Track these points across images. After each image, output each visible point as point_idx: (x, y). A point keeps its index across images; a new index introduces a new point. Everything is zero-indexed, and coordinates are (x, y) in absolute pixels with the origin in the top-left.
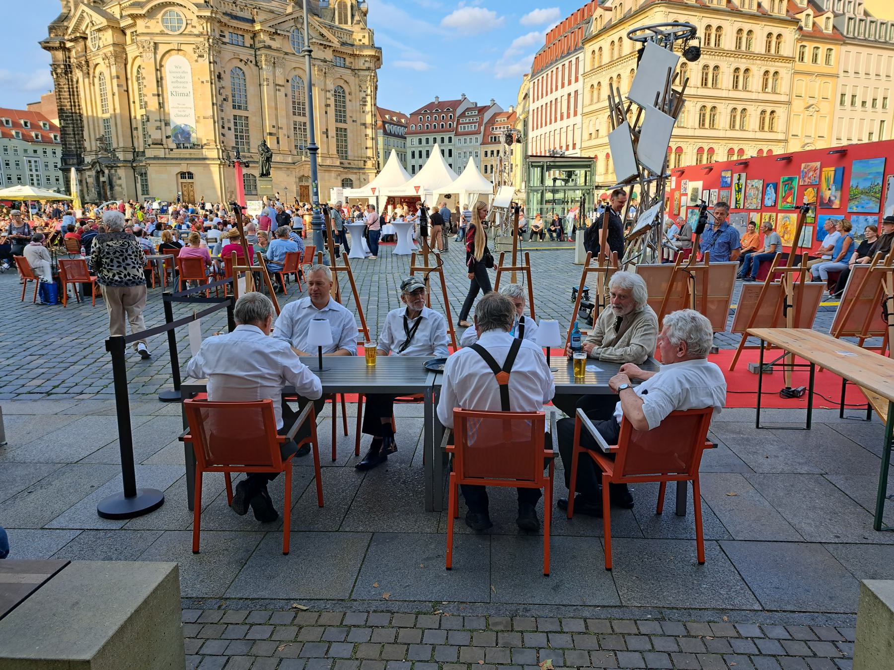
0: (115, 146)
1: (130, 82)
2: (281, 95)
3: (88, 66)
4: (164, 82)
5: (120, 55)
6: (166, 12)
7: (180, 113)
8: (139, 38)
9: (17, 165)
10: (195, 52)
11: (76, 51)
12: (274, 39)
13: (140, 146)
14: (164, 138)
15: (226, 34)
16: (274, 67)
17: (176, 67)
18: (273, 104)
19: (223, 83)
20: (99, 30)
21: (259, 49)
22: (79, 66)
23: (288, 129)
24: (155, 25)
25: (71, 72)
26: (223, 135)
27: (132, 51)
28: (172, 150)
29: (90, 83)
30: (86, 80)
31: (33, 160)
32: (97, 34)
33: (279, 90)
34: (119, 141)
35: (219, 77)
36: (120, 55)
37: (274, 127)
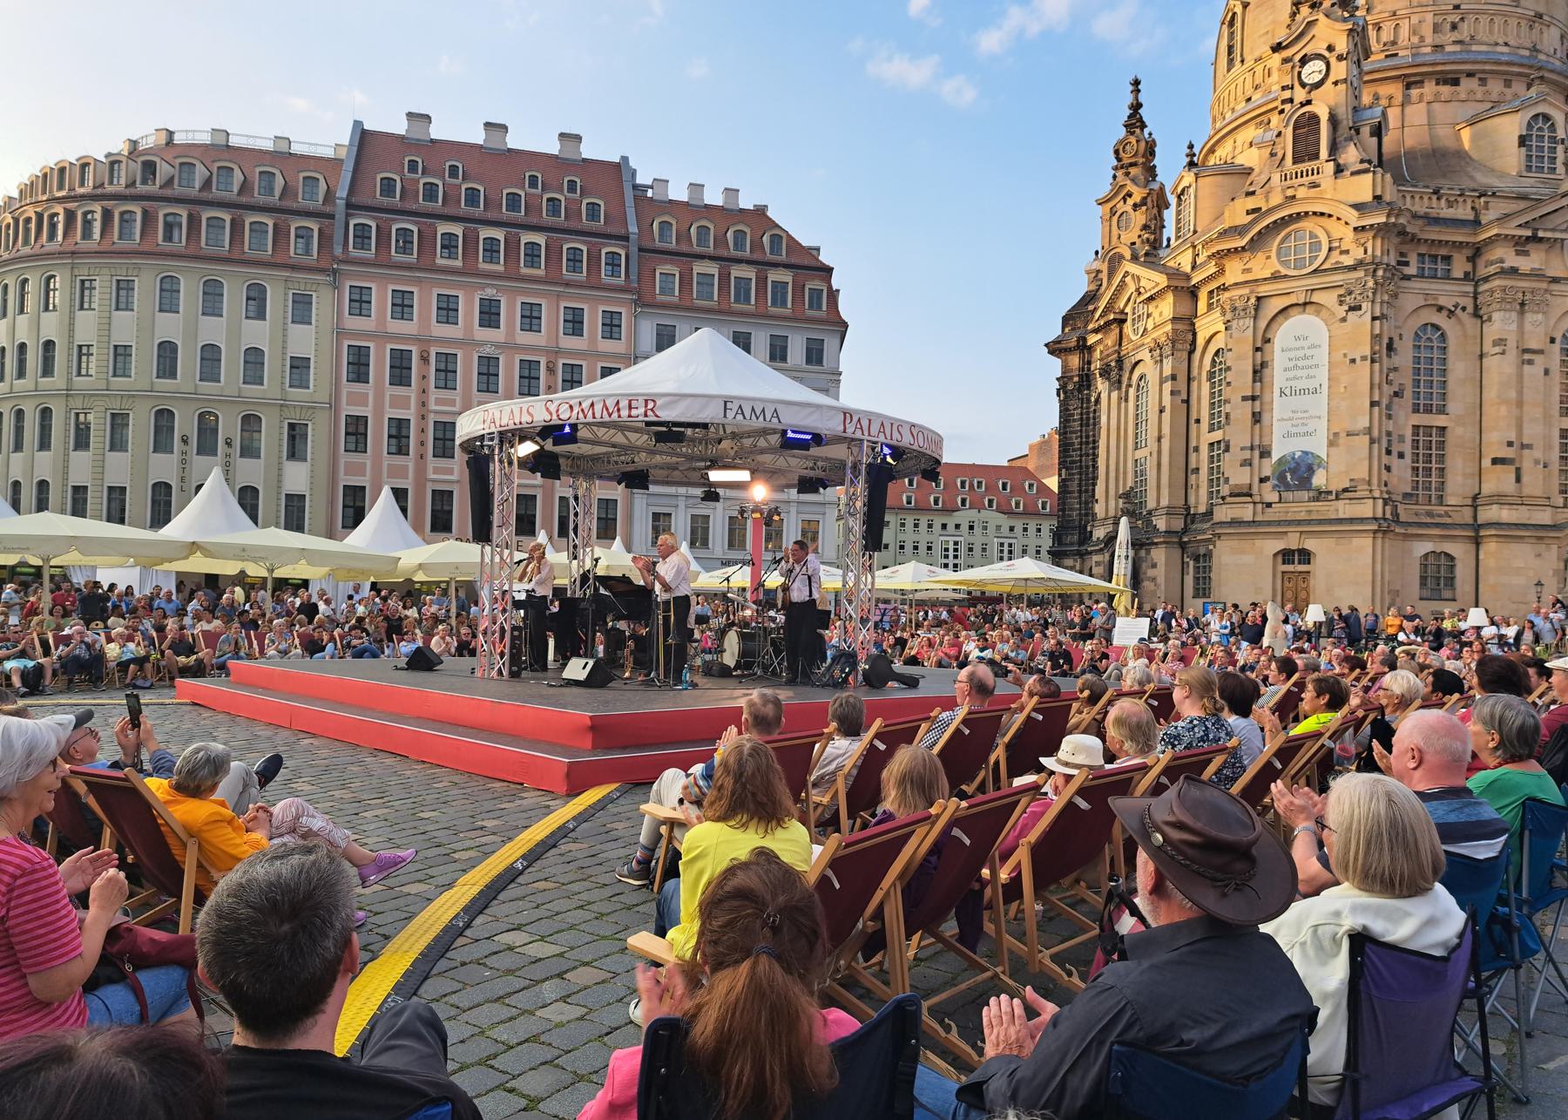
0: (1151, 504)
1: (1194, 385)
2: (1534, 372)
3: (1121, 369)
4: (1266, 372)
5: (1184, 334)
6: (1289, 235)
7: (1294, 430)
8: (1227, 295)
9: (984, 550)
10: (1341, 303)
11: (1102, 344)
12: (1526, 253)
13: (1200, 501)
14: (1256, 480)
15: (1413, 259)
16: (1522, 312)
17: (1297, 338)
18: (1513, 394)
19: (1396, 360)
20: (1151, 299)
21: (1486, 279)
22: (1105, 372)
23: (1548, 447)
24: (1262, 265)
25: (1089, 387)
26: (1388, 469)
27: (1209, 324)
28: (1269, 505)
29: (1120, 398)
30: (1115, 395)
31: (1006, 541)
32: (1142, 309)
33: (1530, 362)
34: (1159, 496)
35: (1390, 348)
36: (1184, 334)
37: (1510, 444)
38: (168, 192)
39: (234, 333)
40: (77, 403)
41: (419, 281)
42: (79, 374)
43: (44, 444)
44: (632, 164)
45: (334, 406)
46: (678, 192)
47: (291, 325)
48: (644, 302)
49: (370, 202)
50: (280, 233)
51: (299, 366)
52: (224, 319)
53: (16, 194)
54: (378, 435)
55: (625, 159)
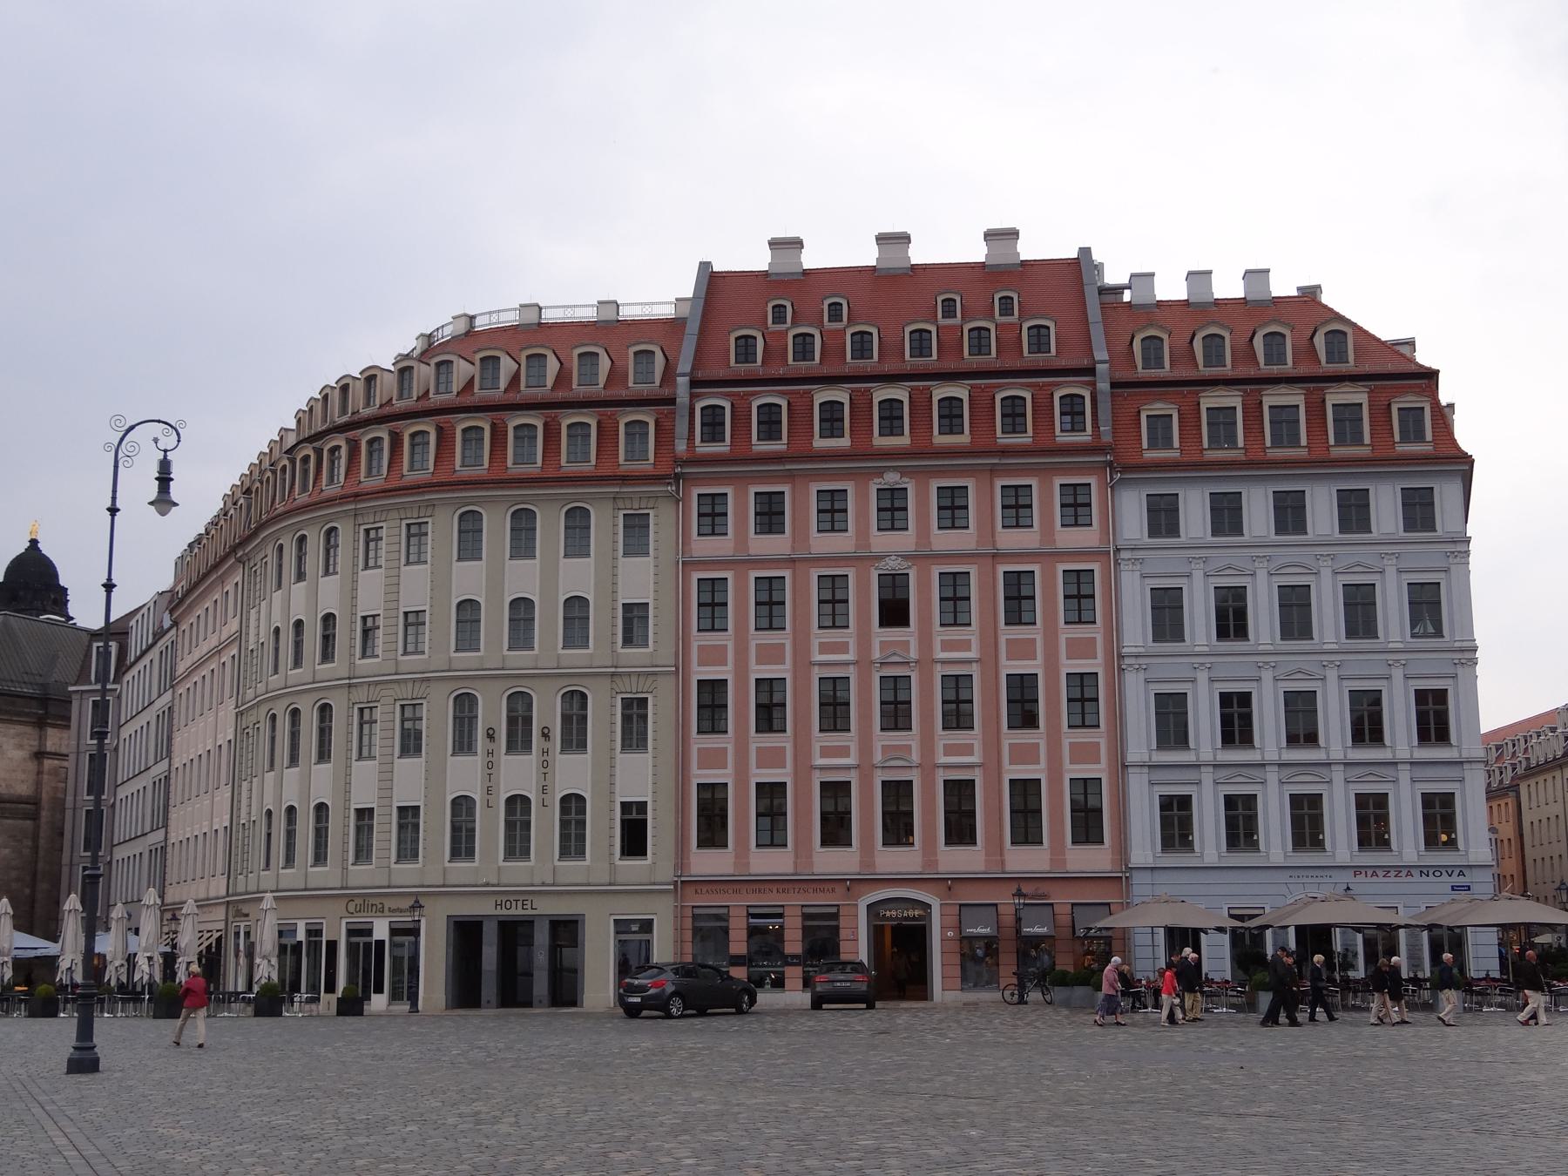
38: (468, 400)
39: (549, 577)
40: (361, 695)
41: (790, 477)
42: (364, 656)
43: (324, 755)
44: (1097, 257)
45: (680, 669)
46: (1170, 288)
47: (623, 562)
48: (1123, 467)
49: (721, 374)
50: (607, 435)
51: (634, 618)
52: (537, 561)
53: (293, 425)
54: (741, 706)
55: (1085, 252)
